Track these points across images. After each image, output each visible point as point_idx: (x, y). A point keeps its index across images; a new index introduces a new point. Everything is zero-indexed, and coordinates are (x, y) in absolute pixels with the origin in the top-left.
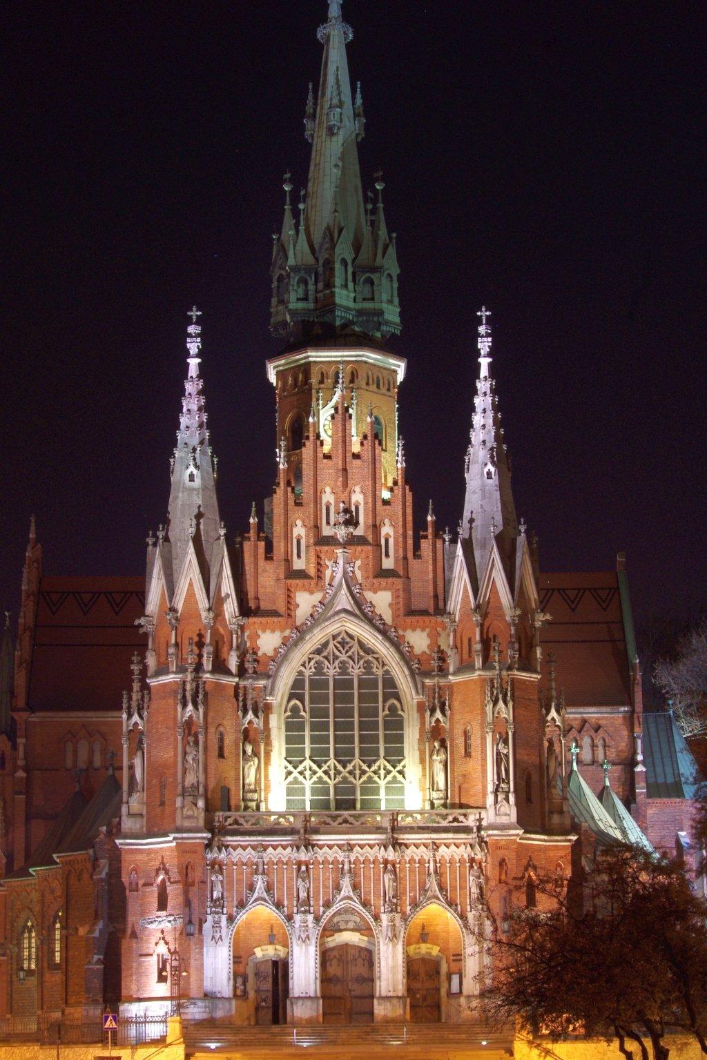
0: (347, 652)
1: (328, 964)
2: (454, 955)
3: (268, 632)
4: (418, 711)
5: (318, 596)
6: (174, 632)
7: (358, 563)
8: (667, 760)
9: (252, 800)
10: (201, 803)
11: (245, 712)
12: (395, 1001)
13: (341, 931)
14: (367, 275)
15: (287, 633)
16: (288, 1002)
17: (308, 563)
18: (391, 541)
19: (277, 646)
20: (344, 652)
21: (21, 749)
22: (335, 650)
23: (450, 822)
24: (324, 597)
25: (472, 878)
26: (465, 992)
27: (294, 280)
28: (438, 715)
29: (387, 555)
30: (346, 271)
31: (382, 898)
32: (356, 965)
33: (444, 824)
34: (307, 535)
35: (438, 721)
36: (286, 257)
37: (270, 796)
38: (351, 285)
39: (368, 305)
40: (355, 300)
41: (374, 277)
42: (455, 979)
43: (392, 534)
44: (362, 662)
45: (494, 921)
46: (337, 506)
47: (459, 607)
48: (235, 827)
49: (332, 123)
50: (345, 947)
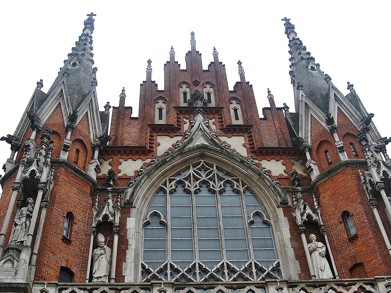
0: (207, 176)
3: (130, 161)
15: (148, 161)
18: (239, 112)
19: (138, 168)
20: (204, 176)
22: (195, 174)
28: (309, 211)
35: (309, 216)
43: (238, 106)
44: (222, 183)
47: (309, 134)
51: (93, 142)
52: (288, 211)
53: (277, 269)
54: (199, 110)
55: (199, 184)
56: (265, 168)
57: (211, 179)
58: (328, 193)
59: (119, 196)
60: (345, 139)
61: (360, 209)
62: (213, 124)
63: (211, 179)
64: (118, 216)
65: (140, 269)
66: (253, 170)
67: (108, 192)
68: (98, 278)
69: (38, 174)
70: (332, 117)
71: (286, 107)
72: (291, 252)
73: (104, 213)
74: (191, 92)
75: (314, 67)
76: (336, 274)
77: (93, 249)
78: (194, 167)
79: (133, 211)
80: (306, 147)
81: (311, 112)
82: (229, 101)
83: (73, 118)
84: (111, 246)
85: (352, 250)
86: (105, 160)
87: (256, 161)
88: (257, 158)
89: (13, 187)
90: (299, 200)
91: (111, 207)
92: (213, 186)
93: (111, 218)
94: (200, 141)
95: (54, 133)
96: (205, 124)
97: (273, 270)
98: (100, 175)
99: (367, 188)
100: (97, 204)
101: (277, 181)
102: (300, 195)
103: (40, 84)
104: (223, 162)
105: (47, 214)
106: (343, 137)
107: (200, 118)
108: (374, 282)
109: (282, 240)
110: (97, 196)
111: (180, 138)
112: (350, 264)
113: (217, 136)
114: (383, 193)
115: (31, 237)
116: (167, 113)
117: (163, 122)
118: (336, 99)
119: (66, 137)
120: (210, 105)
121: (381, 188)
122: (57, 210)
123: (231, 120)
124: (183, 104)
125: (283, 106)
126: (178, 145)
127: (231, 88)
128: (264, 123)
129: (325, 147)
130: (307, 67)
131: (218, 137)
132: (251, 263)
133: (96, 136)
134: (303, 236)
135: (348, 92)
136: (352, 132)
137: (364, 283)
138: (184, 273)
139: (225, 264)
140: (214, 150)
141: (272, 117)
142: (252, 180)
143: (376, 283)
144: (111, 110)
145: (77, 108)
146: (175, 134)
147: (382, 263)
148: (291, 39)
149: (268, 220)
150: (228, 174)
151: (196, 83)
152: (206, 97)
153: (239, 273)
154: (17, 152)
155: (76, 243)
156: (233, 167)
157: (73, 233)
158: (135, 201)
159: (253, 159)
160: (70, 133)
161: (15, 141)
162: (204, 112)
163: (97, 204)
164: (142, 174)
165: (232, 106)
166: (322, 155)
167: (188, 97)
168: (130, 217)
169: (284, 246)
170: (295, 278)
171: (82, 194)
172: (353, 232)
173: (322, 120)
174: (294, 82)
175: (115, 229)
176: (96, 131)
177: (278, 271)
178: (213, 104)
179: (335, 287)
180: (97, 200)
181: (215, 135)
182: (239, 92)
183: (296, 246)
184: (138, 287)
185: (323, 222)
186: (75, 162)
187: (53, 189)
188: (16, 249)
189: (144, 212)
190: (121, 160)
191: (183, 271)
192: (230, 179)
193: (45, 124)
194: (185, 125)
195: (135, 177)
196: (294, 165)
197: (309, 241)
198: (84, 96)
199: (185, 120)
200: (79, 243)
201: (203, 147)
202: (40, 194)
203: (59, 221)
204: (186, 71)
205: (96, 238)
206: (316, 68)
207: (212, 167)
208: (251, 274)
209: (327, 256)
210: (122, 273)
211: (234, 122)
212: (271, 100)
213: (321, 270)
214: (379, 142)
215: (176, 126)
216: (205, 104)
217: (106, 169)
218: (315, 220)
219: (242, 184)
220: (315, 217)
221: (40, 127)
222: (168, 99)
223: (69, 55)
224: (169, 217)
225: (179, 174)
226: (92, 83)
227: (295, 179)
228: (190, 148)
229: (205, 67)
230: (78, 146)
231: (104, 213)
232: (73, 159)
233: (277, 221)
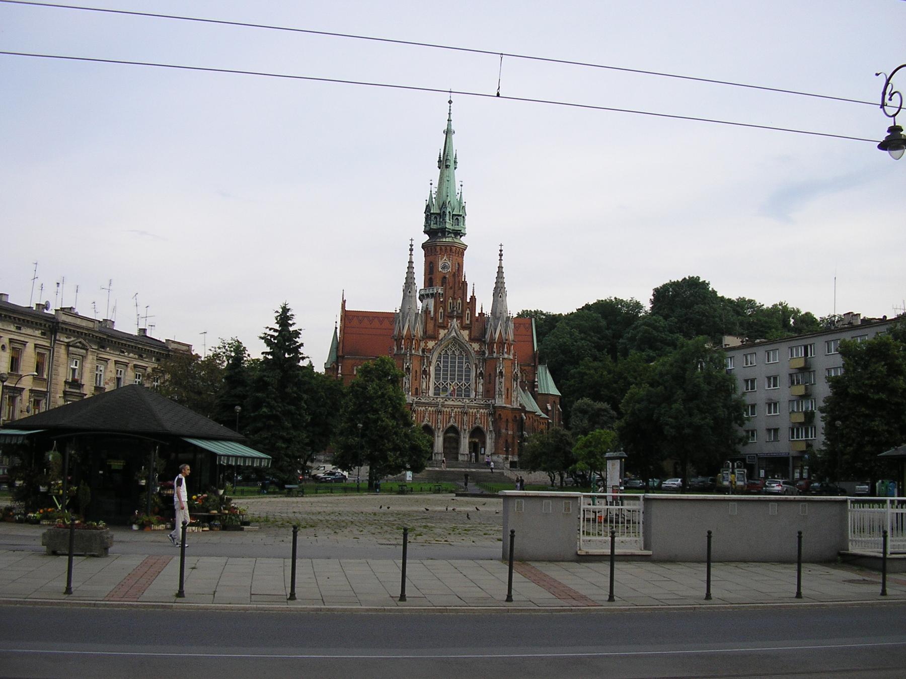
5: (446, 331)
6: (403, 341)
7: (459, 321)
8: (545, 380)
9: (424, 393)
10: (410, 393)
11: (424, 365)
12: (466, 455)
13: (449, 433)
14: (457, 217)
15: (437, 342)
17: (444, 320)
18: (469, 315)
21: (340, 367)
24: (448, 331)
26: (486, 454)
27: (433, 218)
28: (481, 369)
29: (468, 320)
30: (450, 215)
33: (482, 403)
34: (444, 312)
36: (430, 210)
37: (430, 392)
38: (451, 220)
39: (457, 228)
40: (452, 225)
41: (459, 218)
42: (483, 449)
43: (469, 312)
45: (496, 434)
46: (453, 304)
48: (420, 400)
49: (447, 164)
50: (450, 437)
53: (469, 385)
63: (456, 350)
64: (428, 368)
72: (474, 381)
79: (432, 364)
94: (454, 334)
102: (481, 361)
128: (477, 323)
134: (478, 378)
151: (455, 299)
155: (418, 379)
169: (472, 379)
191: (445, 384)
197: (479, 379)
199: (449, 321)
201: (454, 337)
209: (483, 385)
212: (482, 311)
224: (442, 364)
231: (424, 367)
233: (473, 369)
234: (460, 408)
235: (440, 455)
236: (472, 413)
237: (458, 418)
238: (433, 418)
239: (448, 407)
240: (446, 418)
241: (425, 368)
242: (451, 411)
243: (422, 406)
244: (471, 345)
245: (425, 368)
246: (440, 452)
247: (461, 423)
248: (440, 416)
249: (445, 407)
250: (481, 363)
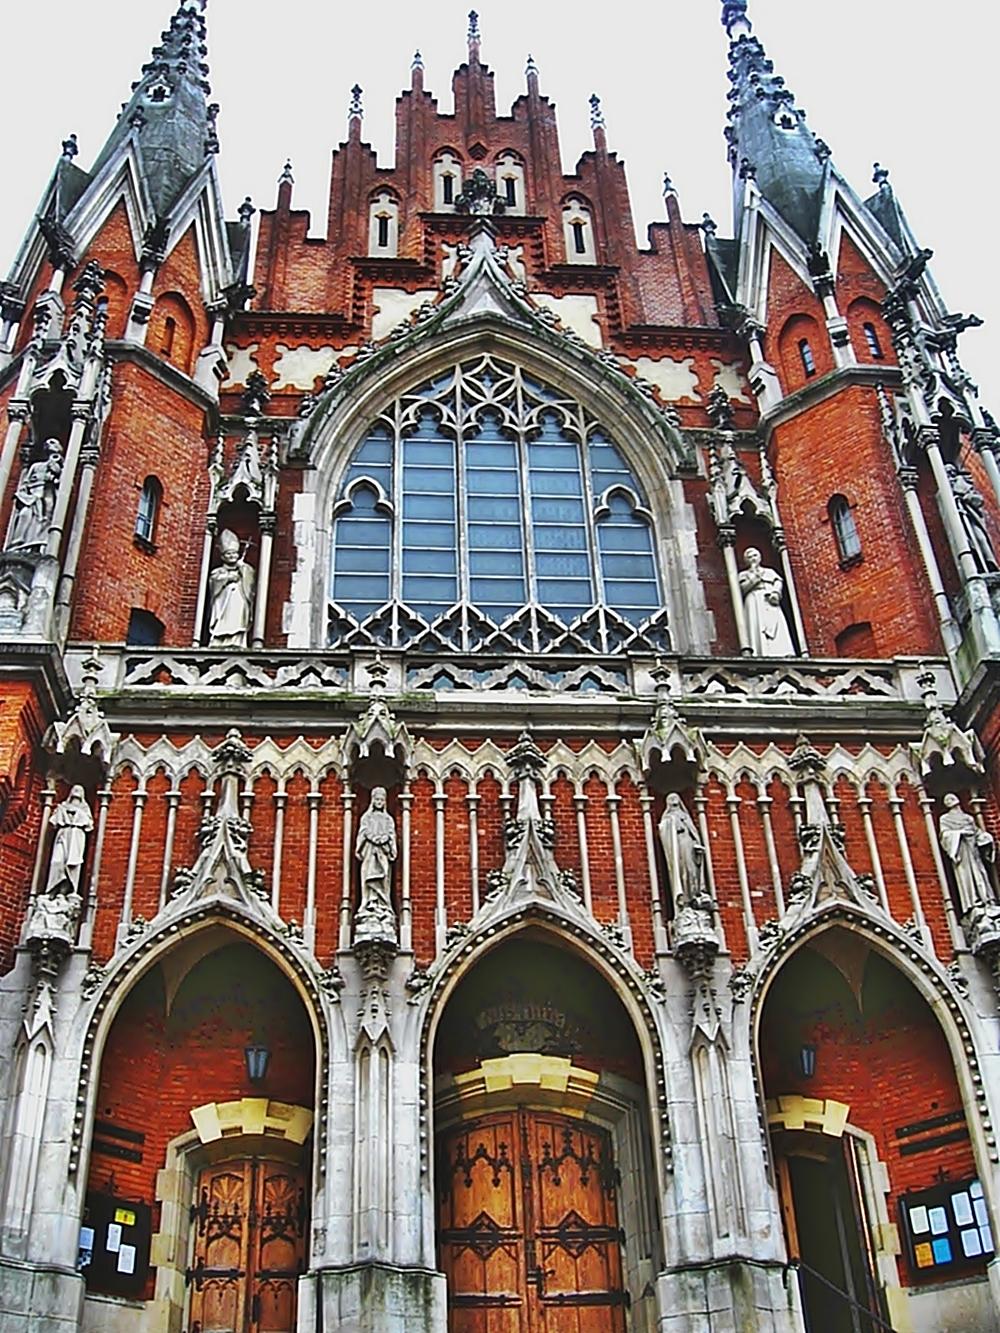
0: (497, 393)
1: (460, 1175)
2: (900, 1134)
4: (687, 502)
16: (305, 1287)
18: (587, 232)
19: (324, 372)
20: (489, 393)
23: (844, 692)
25: (952, 837)
28: (747, 490)
31: (657, 906)
32: (557, 1182)
33: (827, 694)
35: (747, 504)
43: (585, 217)
44: (534, 412)
51: (208, 300)
52: (697, 490)
53: (659, 630)
54: (484, 223)
55: (477, 414)
56: (644, 380)
57: (506, 402)
58: (799, 449)
59: (275, 439)
60: (852, 315)
61: (875, 491)
62: (519, 261)
63: (506, 402)
64: (272, 487)
65: (326, 621)
66: (615, 384)
67: (247, 429)
68: (222, 638)
69: (71, 380)
70: (825, 253)
71: (709, 224)
72: (695, 590)
73: (236, 480)
74: (463, 177)
75: (789, 120)
76: (804, 648)
77: (211, 569)
78: (464, 371)
79: (311, 479)
80: (752, 328)
81: (772, 239)
82: (562, 202)
83: (157, 237)
84: (254, 560)
85: (844, 592)
86: (240, 348)
87: (624, 361)
88: (628, 353)
89: (9, 411)
90: (726, 464)
91: (253, 466)
92: (512, 421)
93: (255, 494)
94: (483, 304)
95: (110, 275)
96: (497, 261)
97: (649, 632)
98: (226, 385)
99: (896, 440)
100: (219, 458)
101: (673, 414)
102: (727, 451)
103: (70, 147)
104: (540, 361)
105: (96, 480)
106: (848, 308)
107: (483, 244)
108: (891, 671)
109: (678, 560)
110: (221, 439)
111: (431, 296)
112: (838, 623)
113: (526, 294)
114: (934, 453)
115: (57, 535)
116: (401, 228)
117: (389, 252)
118: (840, 204)
119: (139, 286)
120: (510, 212)
121: (931, 442)
122: (120, 470)
123: (563, 252)
124: (441, 208)
125: (701, 221)
126: (426, 312)
127: (569, 168)
128: (649, 264)
129: (800, 331)
130: (772, 118)
131: (531, 296)
132: (597, 612)
133: (218, 286)
134: (729, 553)
135: (875, 189)
136: (871, 295)
137: (867, 671)
138: (433, 631)
139: (533, 614)
140: (516, 329)
141: (672, 247)
142: (611, 409)
143: (897, 672)
144: (256, 219)
145: (167, 213)
146: (419, 286)
147: (916, 626)
148: (736, 39)
149: (644, 509)
150: (550, 391)
151: (478, 153)
152: (502, 191)
153: (566, 635)
154: (16, 325)
156: (564, 374)
157: (160, 528)
158: (315, 451)
159: (617, 355)
160: (149, 276)
161: (10, 295)
162: (495, 228)
163: (219, 458)
164: (332, 385)
165: (568, 217)
166: (791, 352)
167: (457, 190)
168: (301, 492)
169: (679, 574)
170: (701, 650)
171: (182, 433)
172: (853, 547)
173: (798, 261)
174: (734, 157)
175: (263, 520)
176: (216, 271)
177: (662, 636)
178: (519, 210)
179: (796, 676)
180: (220, 447)
181: (522, 290)
182: (590, 179)
183: (711, 575)
184: (318, 659)
185: (781, 520)
186: (163, 351)
187: (109, 418)
188: (23, 564)
189: (335, 480)
190: (279, 349)
192: (554, 403)
193: (86, 253)
194: (445, 262)
195: (316, 392)
196: (718, 373)
197: (743, 566)
198: (187, 181)
199: (445, 247)
200: (175, 553)
201: (489, 320)
202: (78, 428)
203: (126, 498)
204: (452, 117)
205: (216, 541)
206: (794, 122)
207: (512, 372)
208: (596, 640)
209: (784, 604)
210: (280, 629)
211: (573, 258)
212: (671, 203)
213: (768, 637)
214: (940, 325)
215: (423, 264)
216: (499, 208)
217: (242, 369)
218: (761, 515)
219: (586, 418)
220: (761, 507)
221: (73, 261)
222: (402, 192)
223: (145, 68)
225: (426, 387)
226: (207, 144)
227: (720, 409)
228: (457, 321)
229: (503, 109)
230: (171, 311)
231: (236, 480)
232: (159, 344)
233: (666, 512)
234: (608, 741)
235: (395, 1294)
236: (746, 786)
237: (600, 841)
238: (296, 850)
239: (472, 740)
240: (457, 842)
241: (242, 489)
242: (503, 774)
243: (180, 735)
244: (629, 371)
245: (242, 489)
246: (407, 1255)
247: (639, 901)
248: (376, 824)
249: (440, 739)
250: (734, 465)
